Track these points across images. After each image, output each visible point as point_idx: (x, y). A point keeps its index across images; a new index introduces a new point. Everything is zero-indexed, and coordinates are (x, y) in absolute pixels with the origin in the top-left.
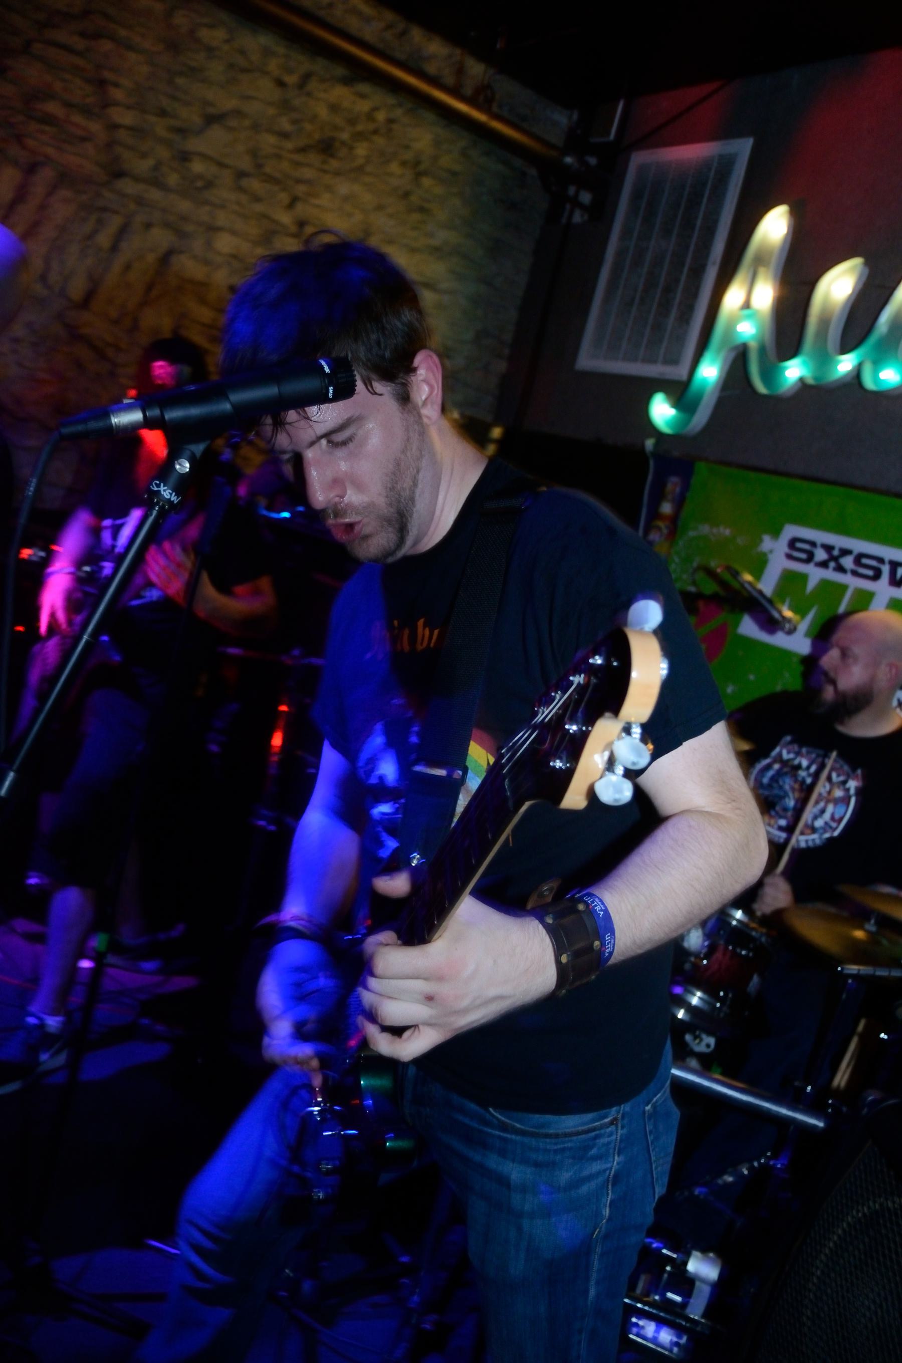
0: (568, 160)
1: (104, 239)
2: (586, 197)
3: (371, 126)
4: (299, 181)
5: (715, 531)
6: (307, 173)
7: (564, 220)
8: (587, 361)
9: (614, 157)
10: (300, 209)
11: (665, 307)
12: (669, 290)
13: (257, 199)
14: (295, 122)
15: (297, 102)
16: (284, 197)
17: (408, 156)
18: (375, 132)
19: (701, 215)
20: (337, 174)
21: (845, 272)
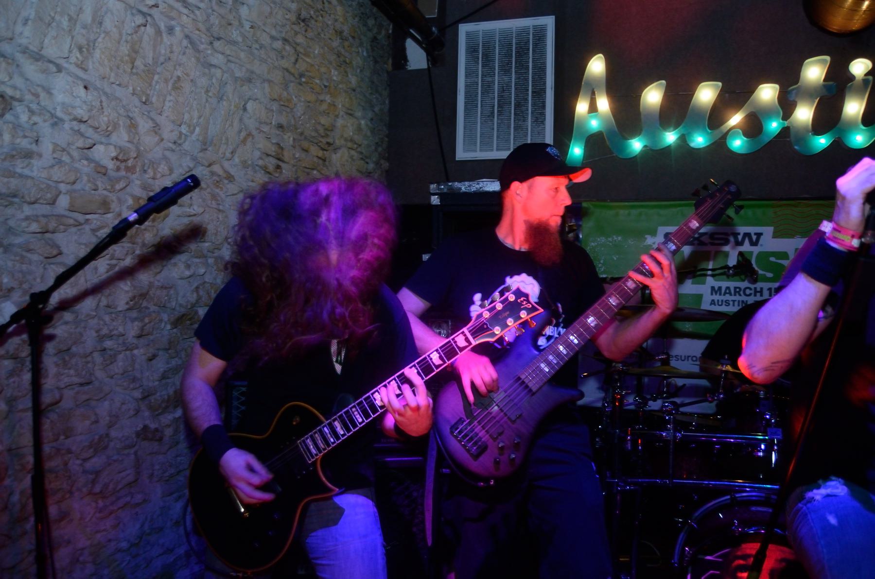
4: (298, 45)
5: (610, 239)
6: (300, 39)
8: (462, 154)
13: (283, 57)
17: (338, 26)
20: (312, 39)
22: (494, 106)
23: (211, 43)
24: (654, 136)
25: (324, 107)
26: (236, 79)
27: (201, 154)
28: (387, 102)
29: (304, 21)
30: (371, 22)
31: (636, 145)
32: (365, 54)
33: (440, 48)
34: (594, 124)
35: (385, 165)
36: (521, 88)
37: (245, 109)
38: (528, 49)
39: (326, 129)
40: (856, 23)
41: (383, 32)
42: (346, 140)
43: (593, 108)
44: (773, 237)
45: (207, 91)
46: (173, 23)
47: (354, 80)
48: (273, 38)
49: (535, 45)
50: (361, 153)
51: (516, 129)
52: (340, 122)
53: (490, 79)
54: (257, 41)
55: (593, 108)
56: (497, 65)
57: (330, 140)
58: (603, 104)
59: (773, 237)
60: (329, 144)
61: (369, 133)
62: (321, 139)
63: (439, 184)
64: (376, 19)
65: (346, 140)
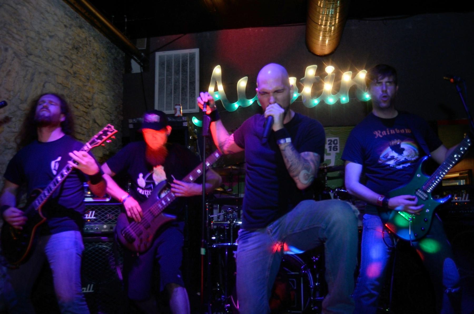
0: (142, 54)
1: (29, 77)
3: (86, 43)
4: (73, 59)
6: (74, 57)
10: (75, 69)
11: (184, 93)
13: (64, 64)
14: (70, 39)
15: (70, 33)
16: (70, 64)
17: (95, 52)
18: (87, 44)
19: (188, 68)
20: (81, 57)
21: (244, 79)
22: (172, 90)
23: (27, 56)
24: (243, 102)
25: (87, 88)
26: (40, 73)
27: (21, 105)
28: (123, 88)
29: (76, 49)
30: (113, 51)
31: (236, 105)
32: (110, 65)
33: (147, 63)
34: (217, 97)
35: (121, 118)
36: (184, 81)
37: (44, 86)
38: (187, 64)
39: (88, 99)
40: (327, 50)
41: (120, 56)
42: (99, 104)
43: (216, 90)
45: (25, 77)
46: (7, 46)
47: (104, 78)
48: (60, 56)
49: (190, 61)
50: (108, 111)
51: (182, 100)
52: (96, 96)
53: (170, 77)
54: (51, 57)
55: (216, 90)
57: (91, 104)
58: (221, 87)
60: (90, 106)
61: (112, 102)
62: (85, 103)
63: (133, 119)
64: (116, 49)
65: (99, 104)
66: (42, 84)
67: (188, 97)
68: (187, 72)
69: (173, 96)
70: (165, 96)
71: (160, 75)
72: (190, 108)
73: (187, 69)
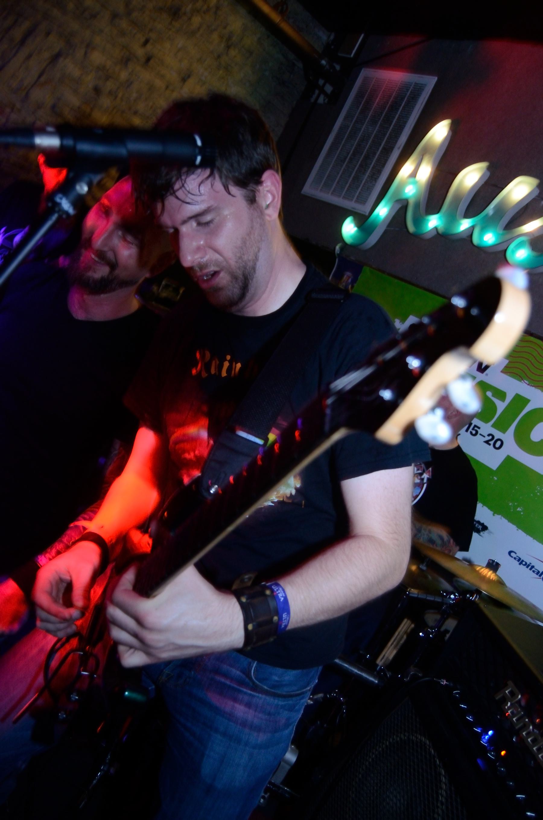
2: (329, 89)
7: (312, 100)
9: (351, 69)
11: (363, 167)
12: (368, 157)
19: (397, 116)
22: (348, 153)
38: (401, 105)
44: (502, 372)
49: (408, 102)
51: (353, 179)
56: (370, 115)
59: (502, 372)
66: (46, 55)
67: (366, 177)
68: (391, 124)
69: (344, 166)
70: (333, 162)
71: (346, 118)
72: (357, 201)
73: (394, 117)
